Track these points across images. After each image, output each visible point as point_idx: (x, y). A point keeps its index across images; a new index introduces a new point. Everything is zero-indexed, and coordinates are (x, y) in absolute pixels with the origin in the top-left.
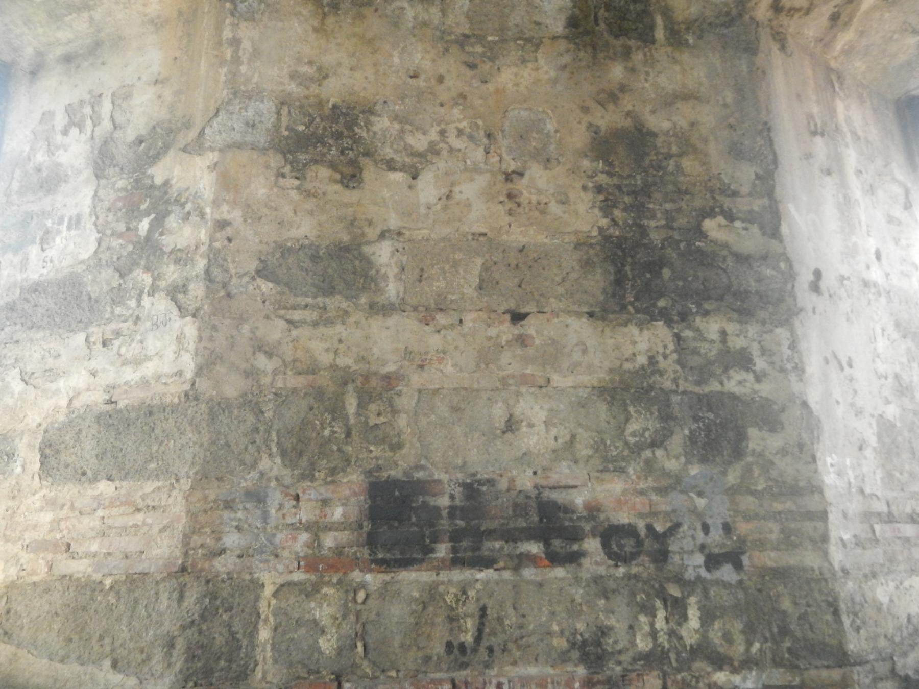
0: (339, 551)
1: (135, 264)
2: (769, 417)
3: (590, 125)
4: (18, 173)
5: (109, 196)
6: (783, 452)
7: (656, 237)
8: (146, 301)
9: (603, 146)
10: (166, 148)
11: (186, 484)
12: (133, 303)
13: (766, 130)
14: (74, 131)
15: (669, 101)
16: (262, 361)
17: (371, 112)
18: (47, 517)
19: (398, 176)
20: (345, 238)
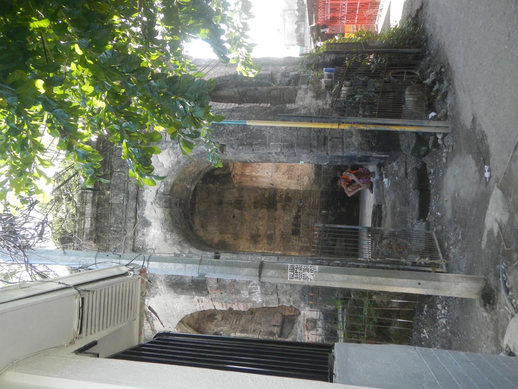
2: (287, 194)
9: (256, 207)
13: (254, 188)
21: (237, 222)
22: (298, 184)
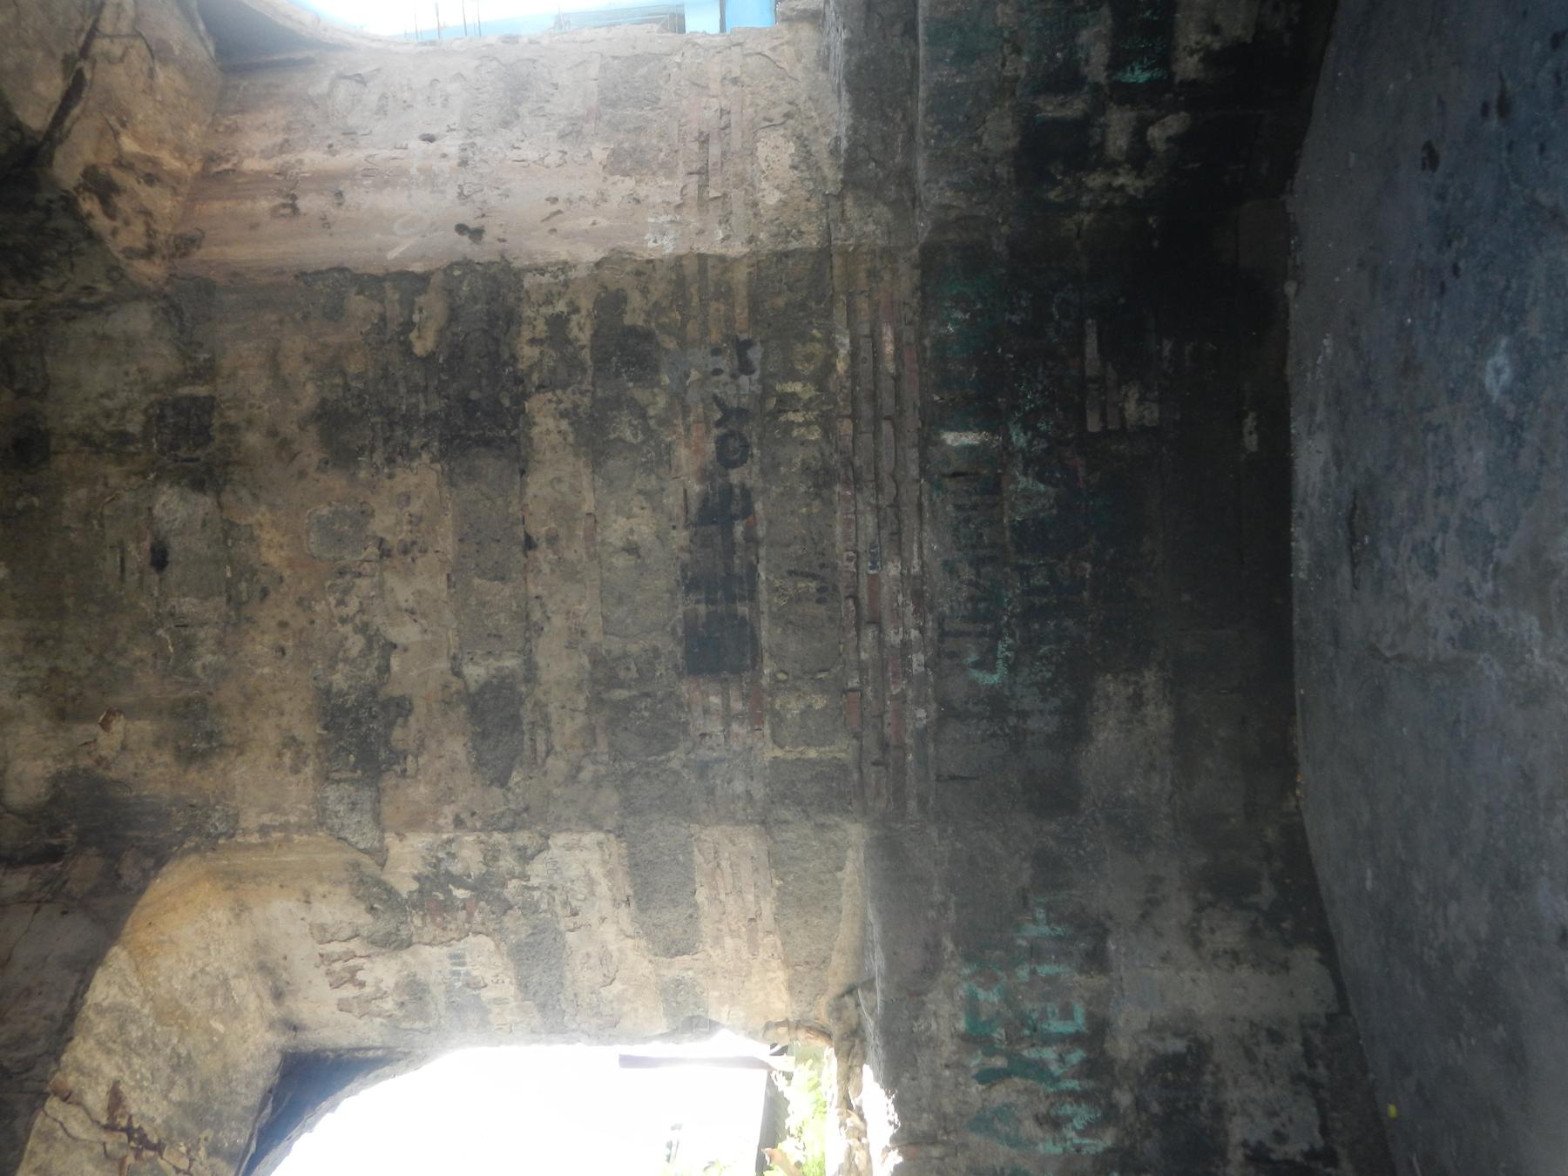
0: (745, 697)
1: (498, 897)
2: (611, 303)
3: (318, 468)
4: (405, 1025)
5: (431, 931)
6: (645, 292)
7: (438, 404)
8: (534, 882)
9: (342, 457)
10: (379, 883)
11: (695, 828)
12: (536, 894)
14: (360, 976)
15: (282, 384)
16: (586, 775)
17: (327, 692)
18: (729, 942)
19: (395, 663)
20: (463, 708)
21: (188, 605)
22: (702, 203)
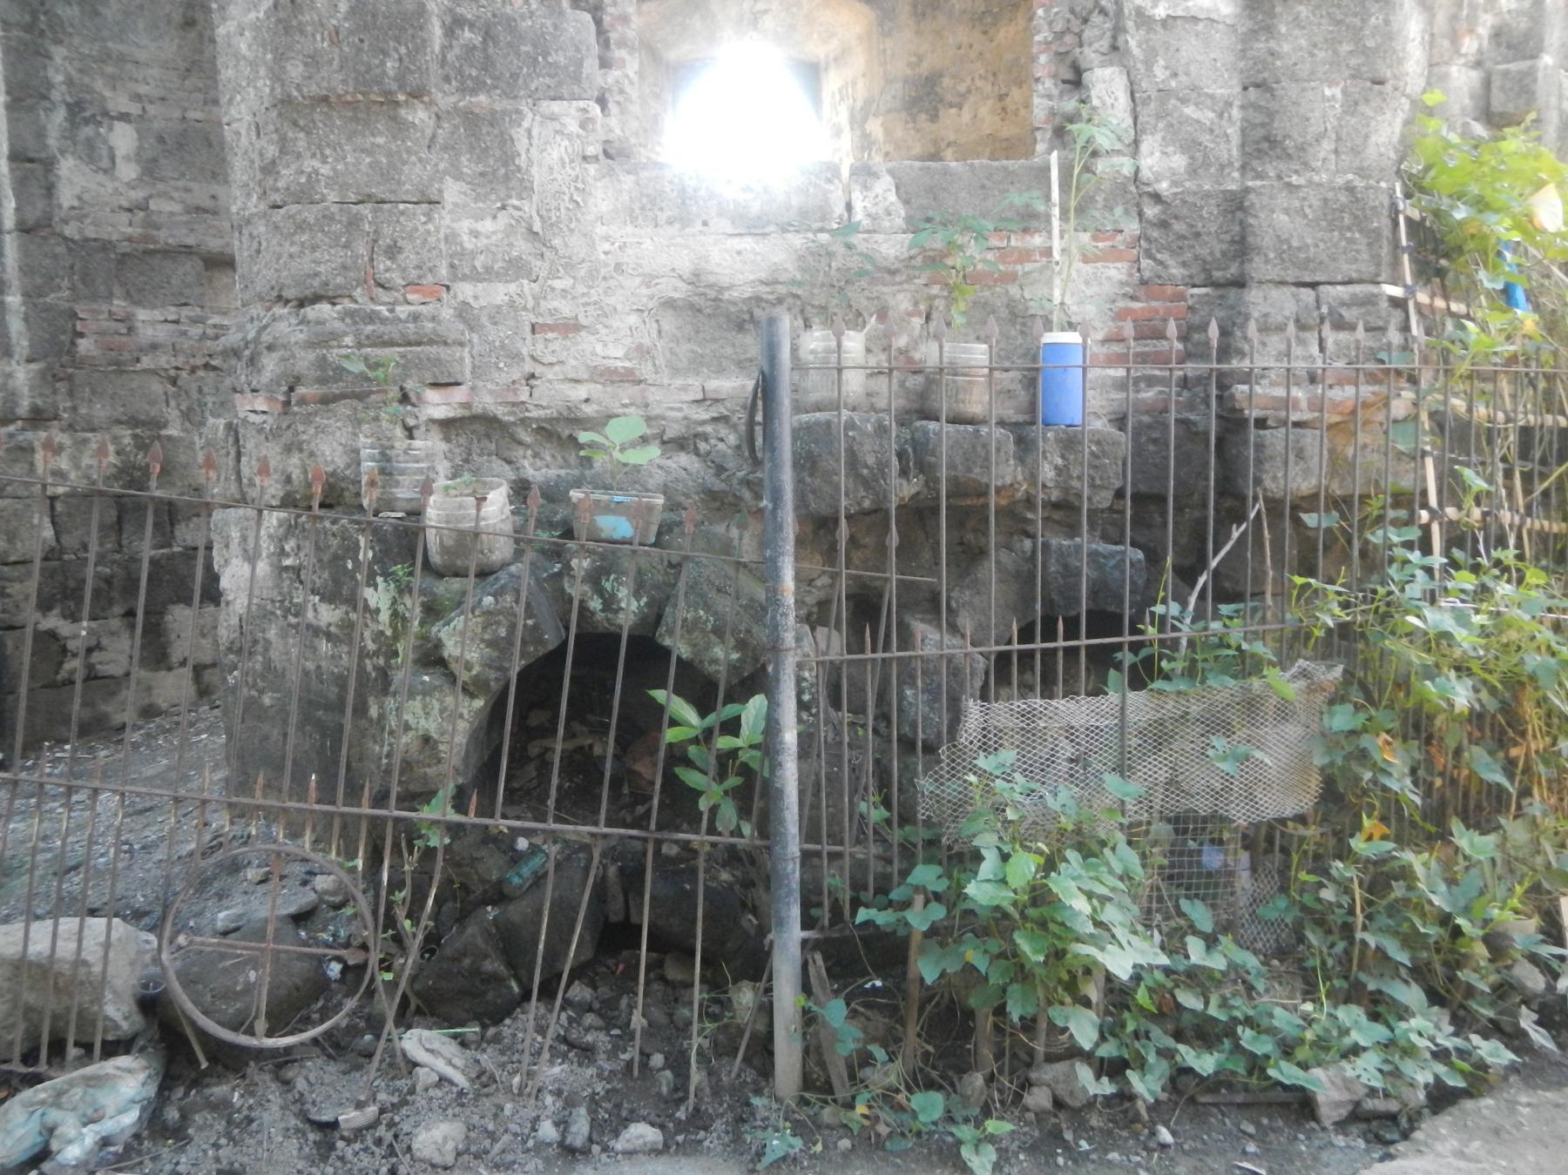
17: (941, 76)
19: (953, 111)
